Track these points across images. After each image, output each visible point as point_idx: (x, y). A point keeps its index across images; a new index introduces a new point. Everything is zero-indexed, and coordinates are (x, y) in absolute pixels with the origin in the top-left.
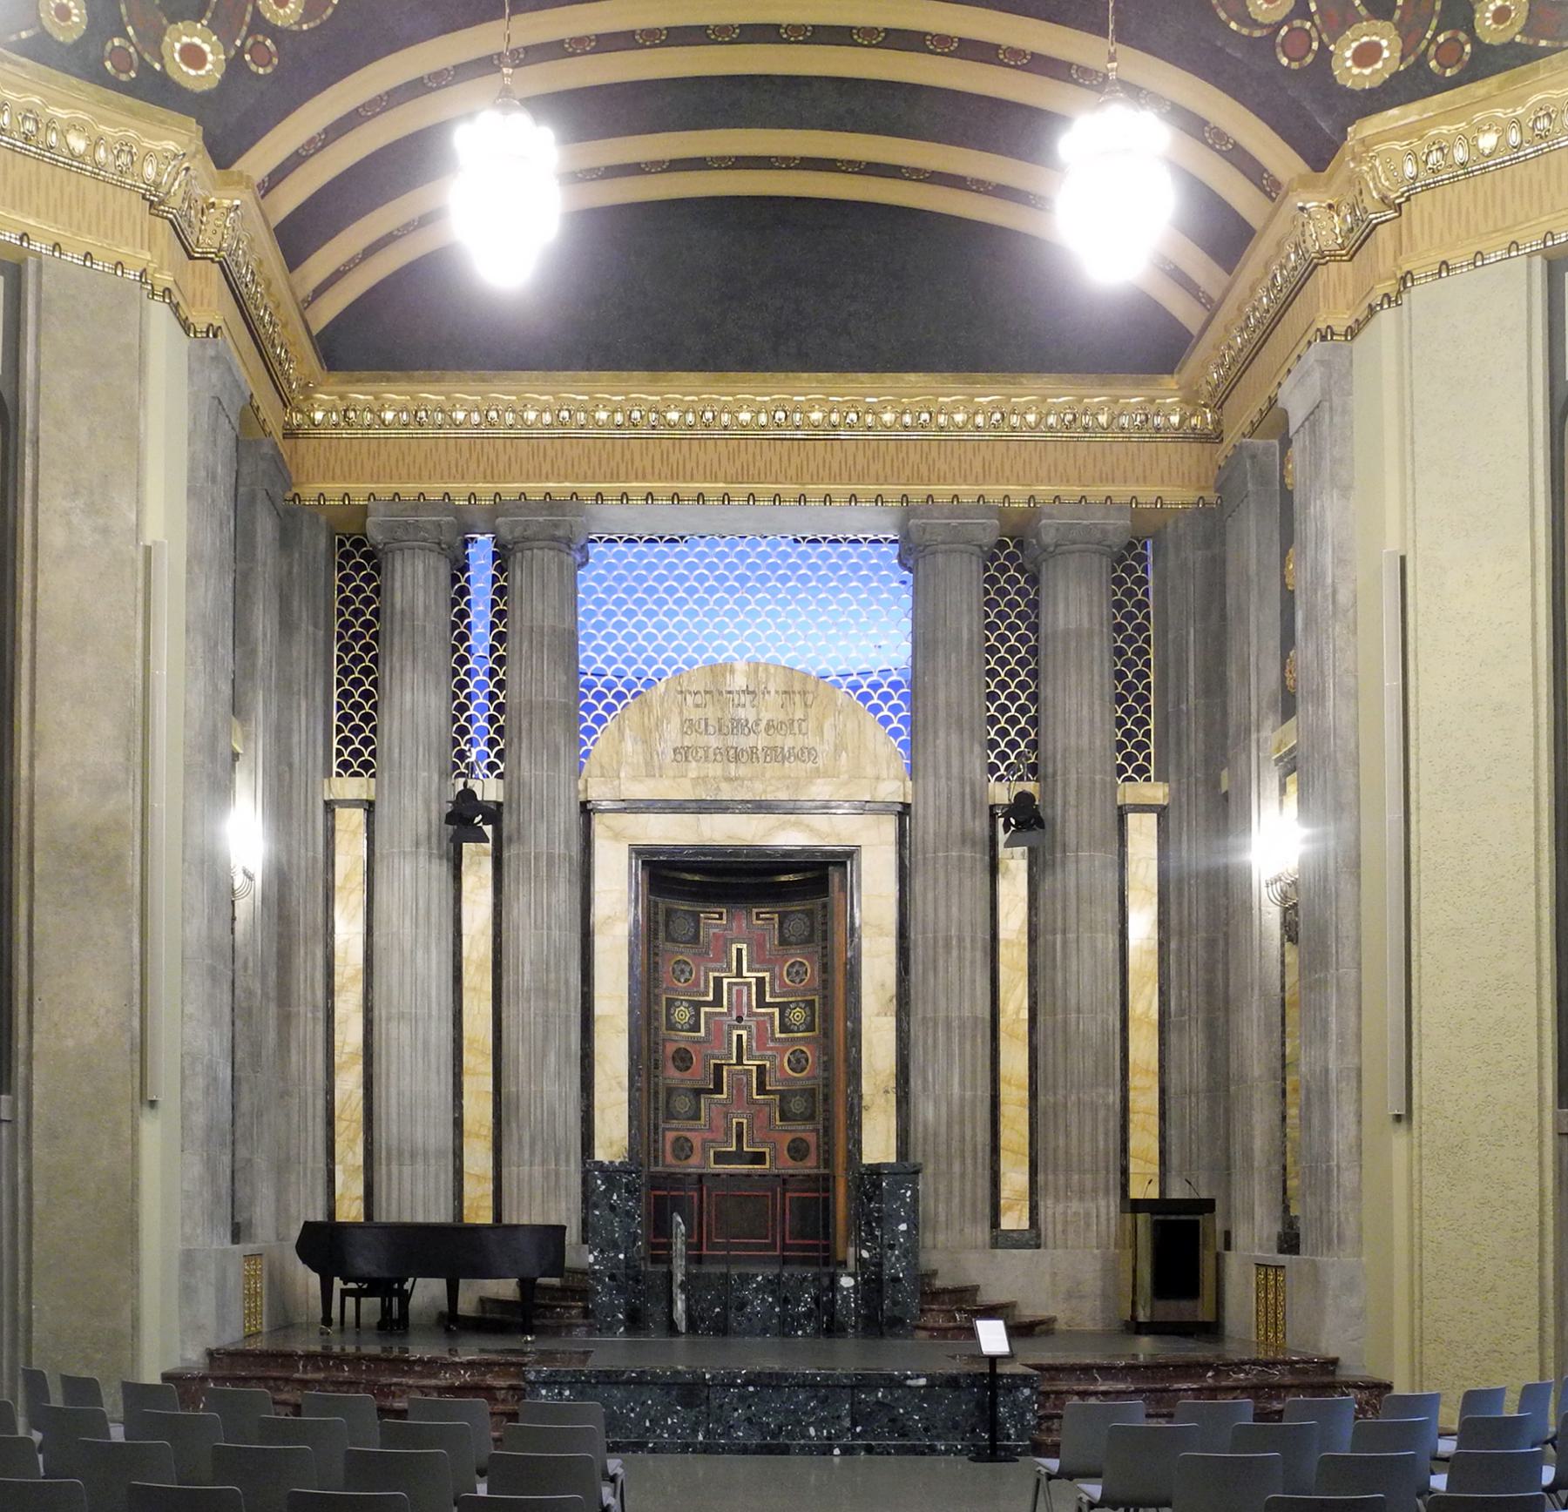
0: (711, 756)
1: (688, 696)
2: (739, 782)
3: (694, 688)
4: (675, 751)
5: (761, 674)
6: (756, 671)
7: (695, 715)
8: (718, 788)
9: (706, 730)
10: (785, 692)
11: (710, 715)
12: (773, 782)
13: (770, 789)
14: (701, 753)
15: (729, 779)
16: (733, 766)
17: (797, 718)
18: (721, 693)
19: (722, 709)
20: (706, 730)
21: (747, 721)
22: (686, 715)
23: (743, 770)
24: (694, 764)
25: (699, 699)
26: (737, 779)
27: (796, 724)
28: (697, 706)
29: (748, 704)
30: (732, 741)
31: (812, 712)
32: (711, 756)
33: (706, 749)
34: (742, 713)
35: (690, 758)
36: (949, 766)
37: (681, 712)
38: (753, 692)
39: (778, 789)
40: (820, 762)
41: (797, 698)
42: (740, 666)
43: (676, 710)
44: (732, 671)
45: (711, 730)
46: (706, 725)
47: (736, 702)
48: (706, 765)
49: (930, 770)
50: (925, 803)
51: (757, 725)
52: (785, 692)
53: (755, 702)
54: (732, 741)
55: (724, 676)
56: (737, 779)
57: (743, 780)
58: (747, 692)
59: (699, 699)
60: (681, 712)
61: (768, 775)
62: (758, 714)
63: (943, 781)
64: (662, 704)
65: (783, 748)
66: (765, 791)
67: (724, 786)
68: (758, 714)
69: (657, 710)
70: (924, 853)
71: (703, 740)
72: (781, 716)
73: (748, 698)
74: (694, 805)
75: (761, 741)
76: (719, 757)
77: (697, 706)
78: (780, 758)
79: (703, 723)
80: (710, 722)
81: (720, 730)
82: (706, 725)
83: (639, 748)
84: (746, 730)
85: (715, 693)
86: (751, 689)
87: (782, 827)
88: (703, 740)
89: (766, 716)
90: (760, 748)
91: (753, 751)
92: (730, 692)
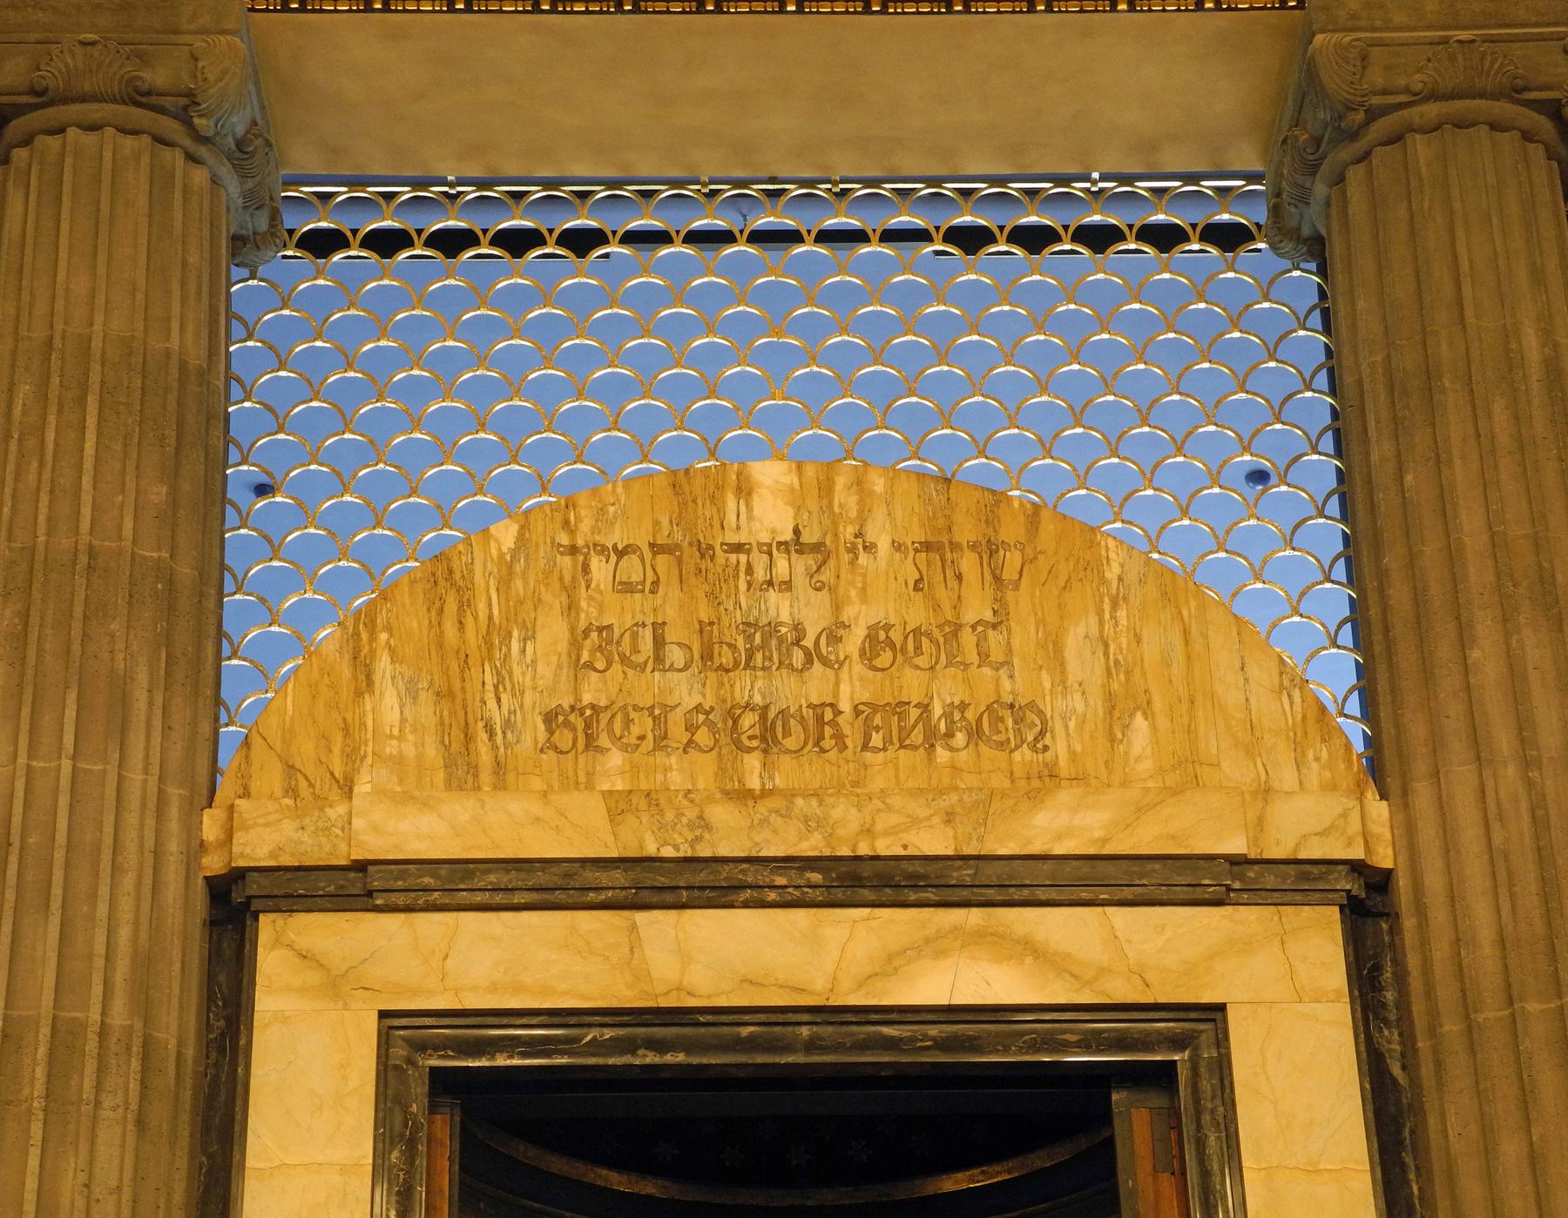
0: (678, 734)
1: (596, 563)
2: (777, 802)
3: (616, 537)
4: (550, 718)
5: (845, 498)
6: (826, 489)
7: (621, 614)
8: (703, 823)
9: (659, 658)
10: (927, 547)
11: (670, 613)
12: (896, 801)
13: (884, 821)
14: (641, 725)
15: (743, 796)
16: (753, 762)
17: (969, 617)
18: (705, 551)
19: (712, 596)
20: (659, 658)
21: (798, 629)
22: (588, 612)
23: (787, 773)
24: (616, 759)
25: (632, 569)
26: (766, 793)
27: (968, 638)
28: (627, 588)
29: (800, 580)
30: (747, 687)
31: (1021, 602)
32: (678, 734)
33: (659, 715)
34: (779, 607)
35: (604, 740)
36: (1524, 725)
37: (571, 608)
38: (817, 548)
39: (915, 821)
40: (1060, 748)
41: (968, 563)
42: (770, 474)
43: (554, 600)
44: (745, 490)
45: (676, 656)
46: (659, 642)
47: (760, 574)
48: (660, 758)
49: (1457, 748)
50: (1449, 849)
51: (834, 639)
52: (927, 547)
53: (826, 575)
54: (747, 687)
55: (716, 500)
56: (766, 793)
57: (790, 795)
58: (796, 545)
59: (632, 569)
60: (571, 608)
61: (878, 783)
62: (837, 608)
63: (1511, 772)
64: (505, 584)
65: (925, 708)
66: (868, 832)
67: (723, 814)
68: (837, 608)
69: (488, 602)
70: (1467, 1008)
71: (647, 687)
72: (918, 615)
73: (802, 563)
74: (618, 877)
75: (852, 688)
76: (703, 737)
77: (627, 588)
78: (917, 736)
79: (647, 635)
80: (670, 635)
81: (707, 655)
82: (659, 642)
83: (426, 711)
84: (798, 657)
85: (691, 558)
86: (809, 537)
87: (935, 947)
88: (647, 687)
89: (861, 617)
90: (845, 706)
91: (822, 720)
92: (738, 548)
